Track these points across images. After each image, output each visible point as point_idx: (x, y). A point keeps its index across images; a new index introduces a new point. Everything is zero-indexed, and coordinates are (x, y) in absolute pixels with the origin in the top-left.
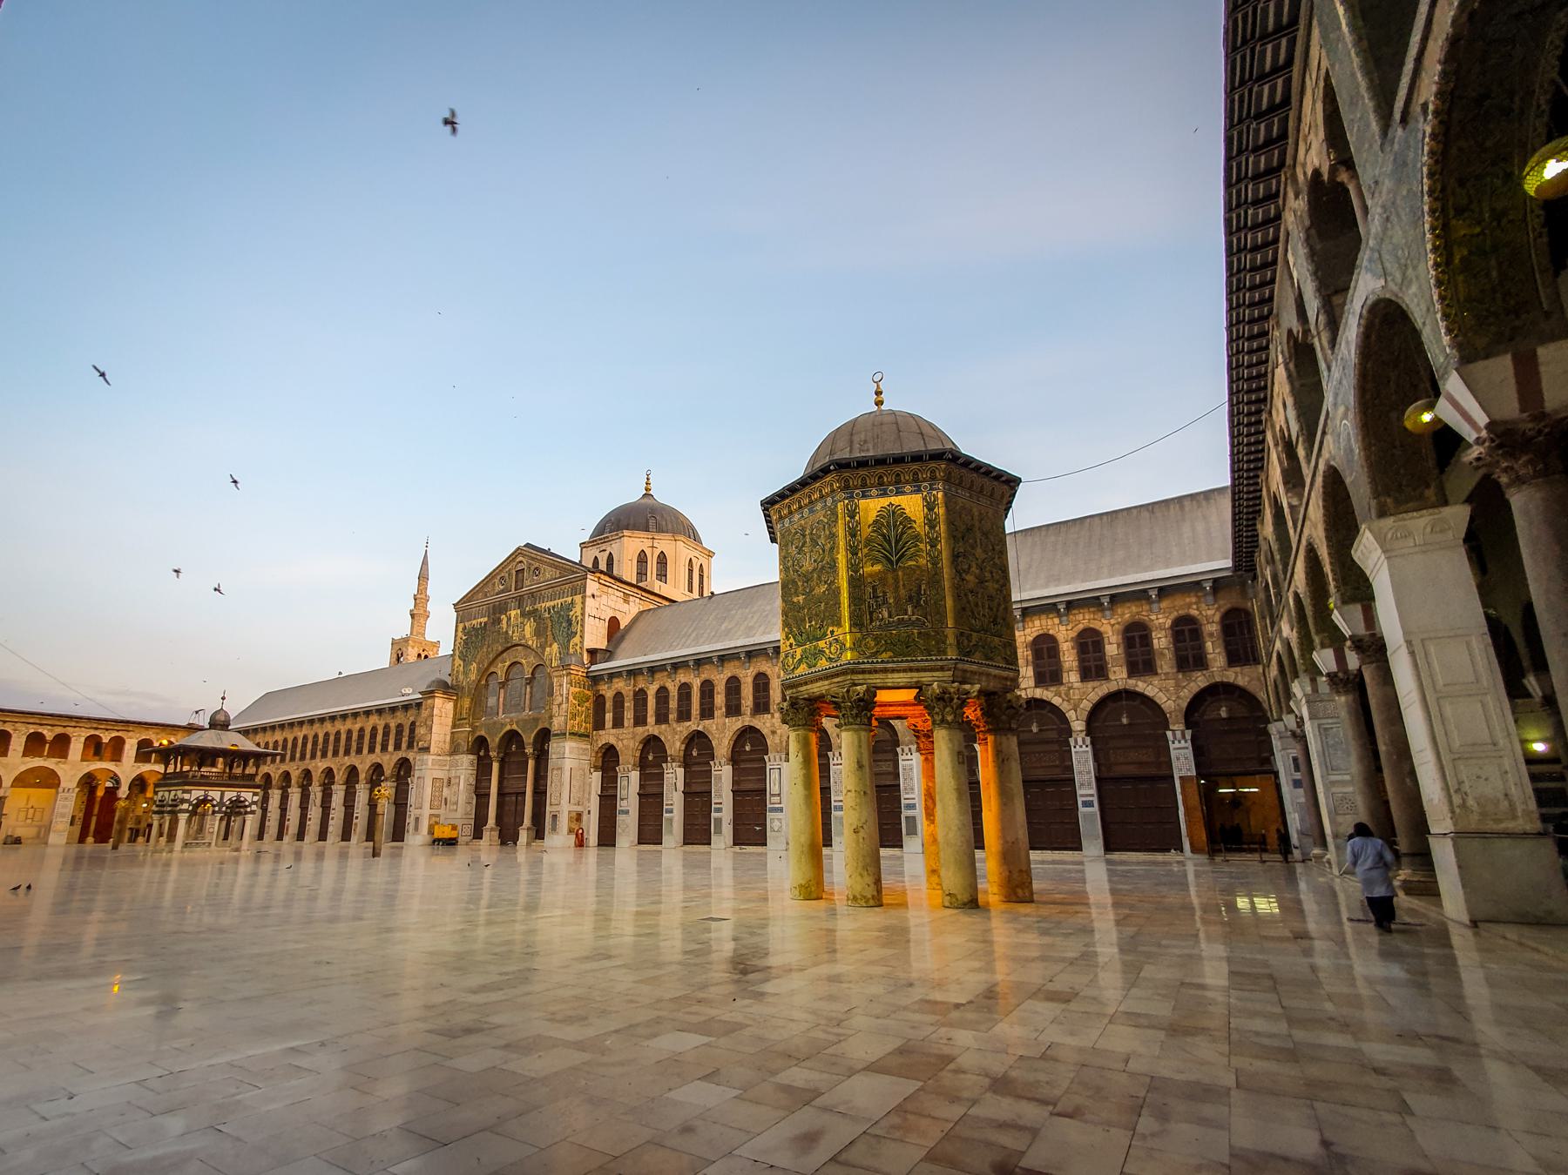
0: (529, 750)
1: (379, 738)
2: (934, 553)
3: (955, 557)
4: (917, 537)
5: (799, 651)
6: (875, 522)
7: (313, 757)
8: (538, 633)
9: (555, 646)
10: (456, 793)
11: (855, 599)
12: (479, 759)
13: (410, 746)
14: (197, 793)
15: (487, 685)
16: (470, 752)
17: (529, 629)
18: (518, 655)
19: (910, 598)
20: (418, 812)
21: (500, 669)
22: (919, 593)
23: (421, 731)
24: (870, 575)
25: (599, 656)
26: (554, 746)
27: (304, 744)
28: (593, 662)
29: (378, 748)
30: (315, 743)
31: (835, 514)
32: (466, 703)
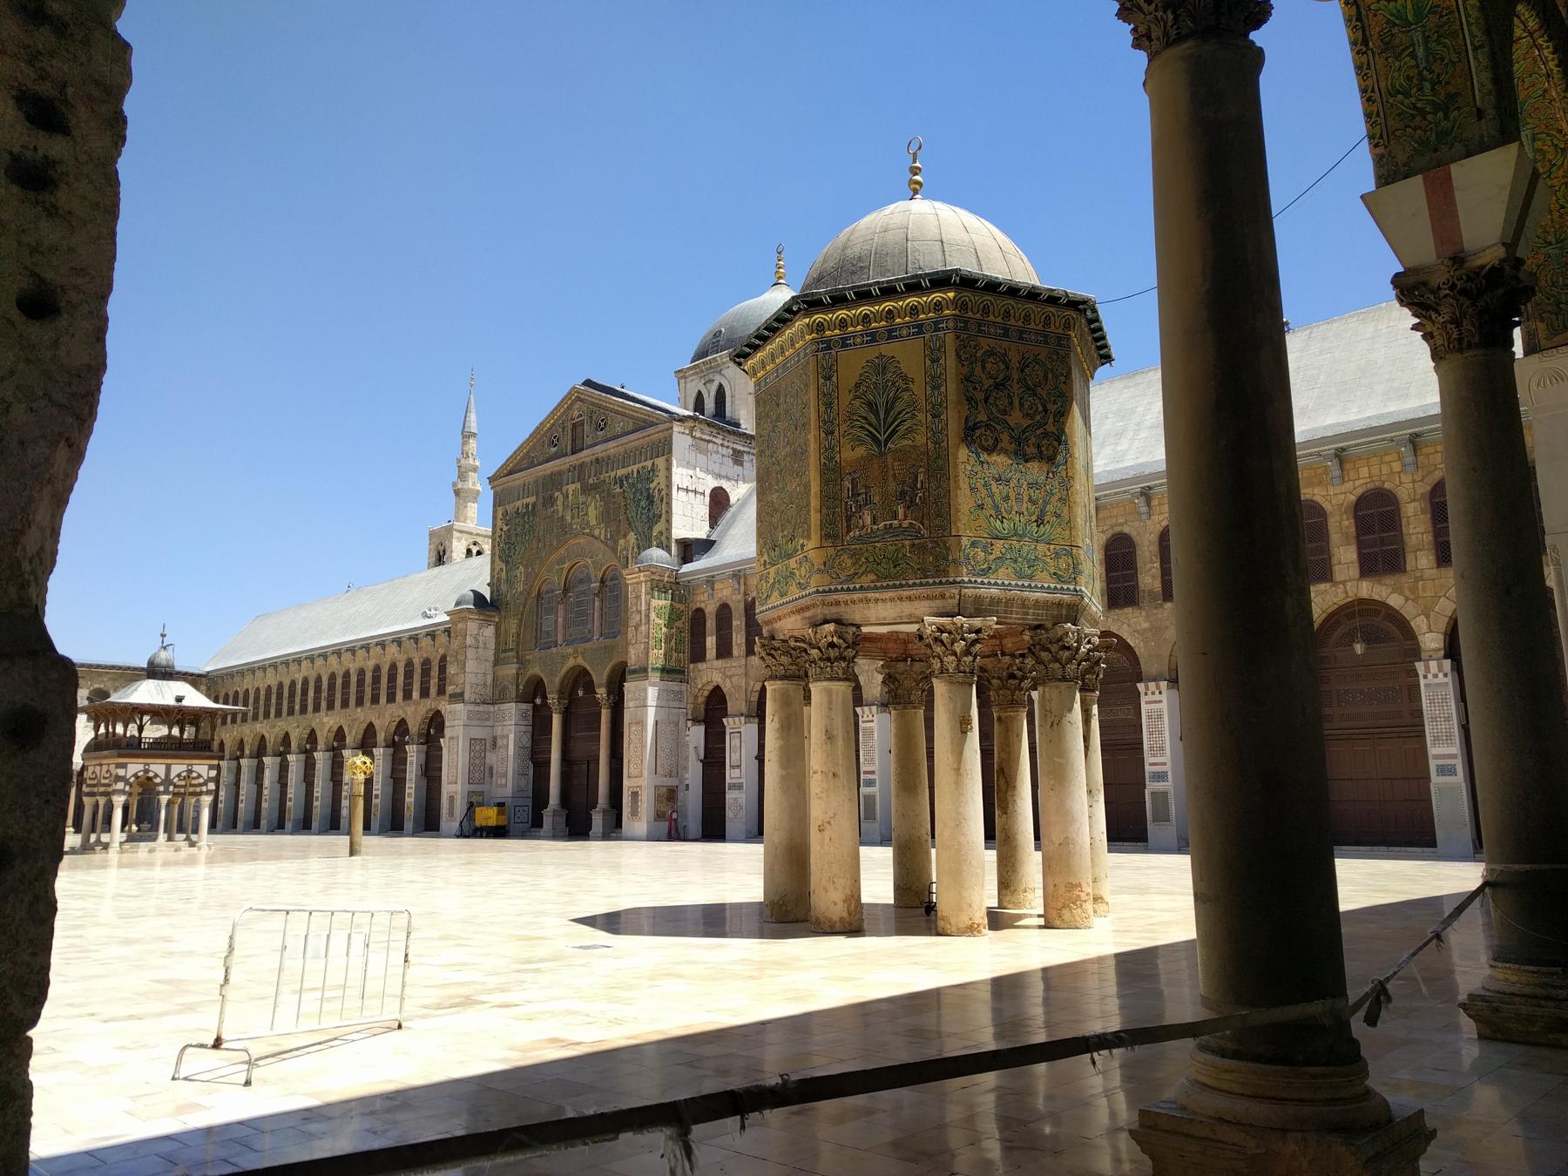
0: (601, 693)
1: (400, 679)
5: (772, 570)
7: (317, 709)
8: (607, 517)
9: (632, 536)
10: (505, 760)
12: (535, 707)
13: (441, 691)
16: (521, 699)
17: (592, 514)
23: (452, 670)
27: (305, 692)
29: (399, 695)
30: (318, 690)
32: (512, 625)
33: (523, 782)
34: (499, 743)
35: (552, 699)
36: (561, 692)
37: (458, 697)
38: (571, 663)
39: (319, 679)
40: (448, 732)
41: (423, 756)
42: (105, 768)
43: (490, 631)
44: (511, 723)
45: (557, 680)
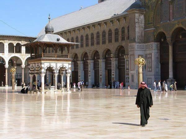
12: (161, 43)
13: (123, 39)
16: (155, 41)
20: (132, 72)
29: (107, 41)
33: (157, 70)
34: (148, 56)
35: (169, 39)
36: (172, 37)
37: (134, 41)
38: (177, 26)
39: (87, 36)
41: (117, 62)
42: (37, 65)
43: (142, 17)
44: (153, 49)
45: (171, 33)
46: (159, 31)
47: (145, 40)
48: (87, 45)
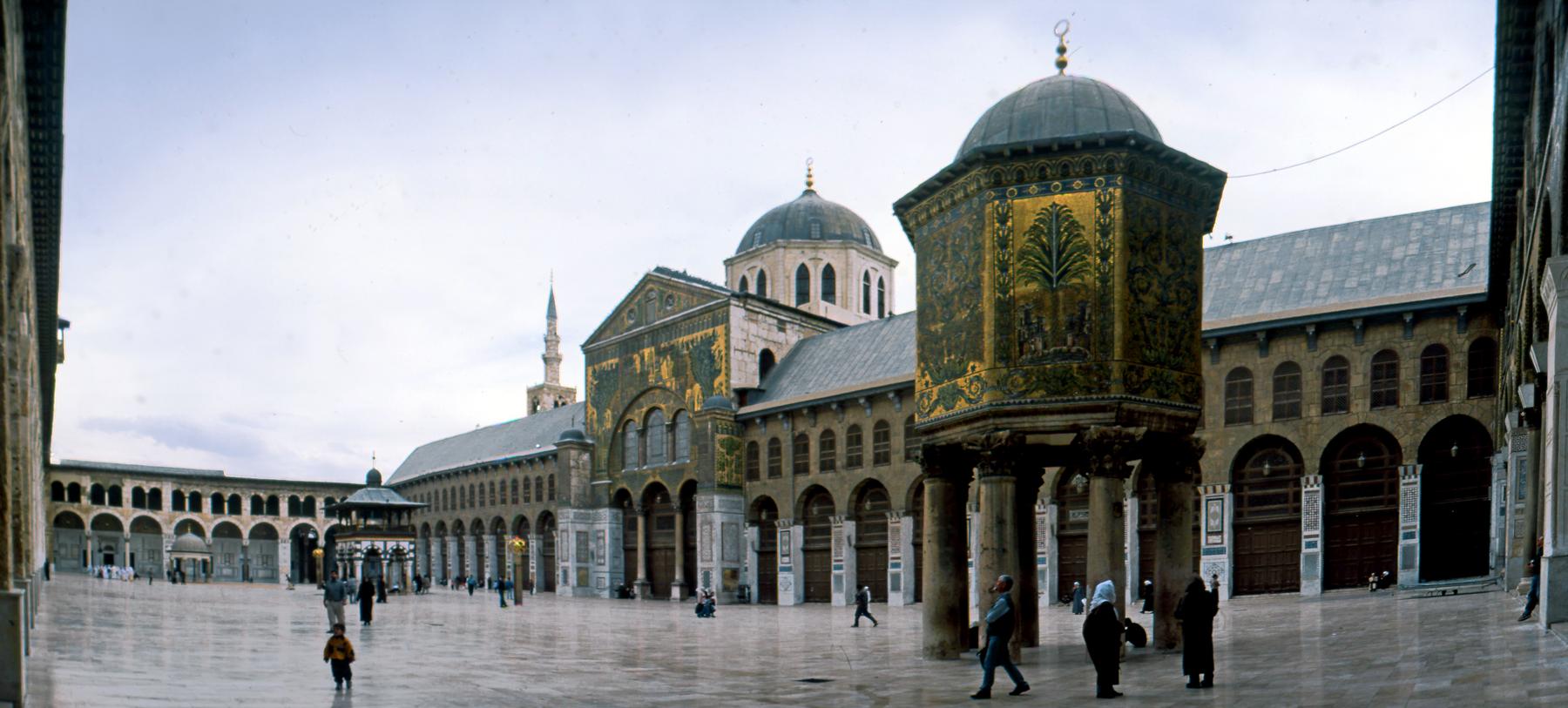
2: (1103, 264)
3: (1131, 273)
4: (1086, 248)
6: (1035, 227)
7: (463, 506)
8: (677, 372)
9: (697, 386)
11: (1003, 328)
13: (551, 497)
14: (365, 544)
15: (624, 434)
17: (666, 367)
18: (657, 399)
19: (1071, 326)
21: (637, 416)
22: (1082, 318)
24: (1024, 297)
25: (748, 397)
26: (701, 500)
27: (454, 495)
28: (742, 403)
29: (521, 500)
30: (463, 495)
31: (981, 218)
32: (603, 453)
37: (567, 504)
38: (651, 480)
40: (561, 527)
43: (586, 457)
44: (605, 521)
46: (621, 485)
47: (591, 501)
48: (482, 504)
